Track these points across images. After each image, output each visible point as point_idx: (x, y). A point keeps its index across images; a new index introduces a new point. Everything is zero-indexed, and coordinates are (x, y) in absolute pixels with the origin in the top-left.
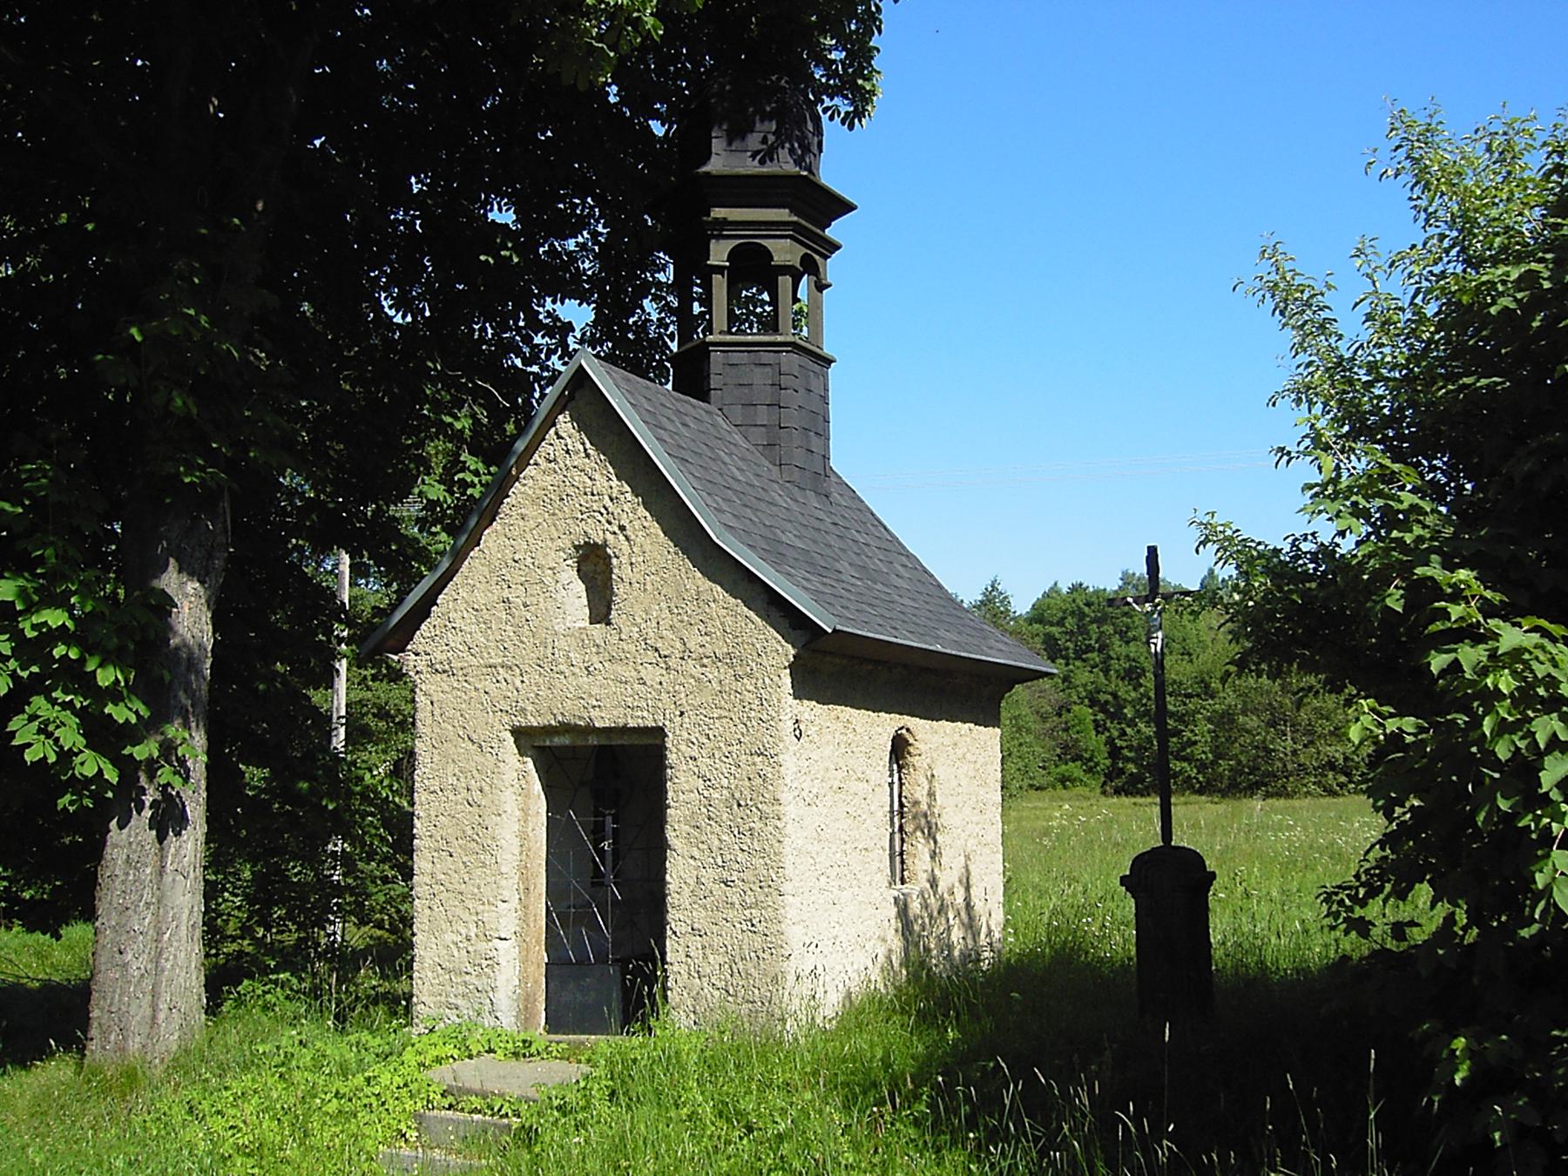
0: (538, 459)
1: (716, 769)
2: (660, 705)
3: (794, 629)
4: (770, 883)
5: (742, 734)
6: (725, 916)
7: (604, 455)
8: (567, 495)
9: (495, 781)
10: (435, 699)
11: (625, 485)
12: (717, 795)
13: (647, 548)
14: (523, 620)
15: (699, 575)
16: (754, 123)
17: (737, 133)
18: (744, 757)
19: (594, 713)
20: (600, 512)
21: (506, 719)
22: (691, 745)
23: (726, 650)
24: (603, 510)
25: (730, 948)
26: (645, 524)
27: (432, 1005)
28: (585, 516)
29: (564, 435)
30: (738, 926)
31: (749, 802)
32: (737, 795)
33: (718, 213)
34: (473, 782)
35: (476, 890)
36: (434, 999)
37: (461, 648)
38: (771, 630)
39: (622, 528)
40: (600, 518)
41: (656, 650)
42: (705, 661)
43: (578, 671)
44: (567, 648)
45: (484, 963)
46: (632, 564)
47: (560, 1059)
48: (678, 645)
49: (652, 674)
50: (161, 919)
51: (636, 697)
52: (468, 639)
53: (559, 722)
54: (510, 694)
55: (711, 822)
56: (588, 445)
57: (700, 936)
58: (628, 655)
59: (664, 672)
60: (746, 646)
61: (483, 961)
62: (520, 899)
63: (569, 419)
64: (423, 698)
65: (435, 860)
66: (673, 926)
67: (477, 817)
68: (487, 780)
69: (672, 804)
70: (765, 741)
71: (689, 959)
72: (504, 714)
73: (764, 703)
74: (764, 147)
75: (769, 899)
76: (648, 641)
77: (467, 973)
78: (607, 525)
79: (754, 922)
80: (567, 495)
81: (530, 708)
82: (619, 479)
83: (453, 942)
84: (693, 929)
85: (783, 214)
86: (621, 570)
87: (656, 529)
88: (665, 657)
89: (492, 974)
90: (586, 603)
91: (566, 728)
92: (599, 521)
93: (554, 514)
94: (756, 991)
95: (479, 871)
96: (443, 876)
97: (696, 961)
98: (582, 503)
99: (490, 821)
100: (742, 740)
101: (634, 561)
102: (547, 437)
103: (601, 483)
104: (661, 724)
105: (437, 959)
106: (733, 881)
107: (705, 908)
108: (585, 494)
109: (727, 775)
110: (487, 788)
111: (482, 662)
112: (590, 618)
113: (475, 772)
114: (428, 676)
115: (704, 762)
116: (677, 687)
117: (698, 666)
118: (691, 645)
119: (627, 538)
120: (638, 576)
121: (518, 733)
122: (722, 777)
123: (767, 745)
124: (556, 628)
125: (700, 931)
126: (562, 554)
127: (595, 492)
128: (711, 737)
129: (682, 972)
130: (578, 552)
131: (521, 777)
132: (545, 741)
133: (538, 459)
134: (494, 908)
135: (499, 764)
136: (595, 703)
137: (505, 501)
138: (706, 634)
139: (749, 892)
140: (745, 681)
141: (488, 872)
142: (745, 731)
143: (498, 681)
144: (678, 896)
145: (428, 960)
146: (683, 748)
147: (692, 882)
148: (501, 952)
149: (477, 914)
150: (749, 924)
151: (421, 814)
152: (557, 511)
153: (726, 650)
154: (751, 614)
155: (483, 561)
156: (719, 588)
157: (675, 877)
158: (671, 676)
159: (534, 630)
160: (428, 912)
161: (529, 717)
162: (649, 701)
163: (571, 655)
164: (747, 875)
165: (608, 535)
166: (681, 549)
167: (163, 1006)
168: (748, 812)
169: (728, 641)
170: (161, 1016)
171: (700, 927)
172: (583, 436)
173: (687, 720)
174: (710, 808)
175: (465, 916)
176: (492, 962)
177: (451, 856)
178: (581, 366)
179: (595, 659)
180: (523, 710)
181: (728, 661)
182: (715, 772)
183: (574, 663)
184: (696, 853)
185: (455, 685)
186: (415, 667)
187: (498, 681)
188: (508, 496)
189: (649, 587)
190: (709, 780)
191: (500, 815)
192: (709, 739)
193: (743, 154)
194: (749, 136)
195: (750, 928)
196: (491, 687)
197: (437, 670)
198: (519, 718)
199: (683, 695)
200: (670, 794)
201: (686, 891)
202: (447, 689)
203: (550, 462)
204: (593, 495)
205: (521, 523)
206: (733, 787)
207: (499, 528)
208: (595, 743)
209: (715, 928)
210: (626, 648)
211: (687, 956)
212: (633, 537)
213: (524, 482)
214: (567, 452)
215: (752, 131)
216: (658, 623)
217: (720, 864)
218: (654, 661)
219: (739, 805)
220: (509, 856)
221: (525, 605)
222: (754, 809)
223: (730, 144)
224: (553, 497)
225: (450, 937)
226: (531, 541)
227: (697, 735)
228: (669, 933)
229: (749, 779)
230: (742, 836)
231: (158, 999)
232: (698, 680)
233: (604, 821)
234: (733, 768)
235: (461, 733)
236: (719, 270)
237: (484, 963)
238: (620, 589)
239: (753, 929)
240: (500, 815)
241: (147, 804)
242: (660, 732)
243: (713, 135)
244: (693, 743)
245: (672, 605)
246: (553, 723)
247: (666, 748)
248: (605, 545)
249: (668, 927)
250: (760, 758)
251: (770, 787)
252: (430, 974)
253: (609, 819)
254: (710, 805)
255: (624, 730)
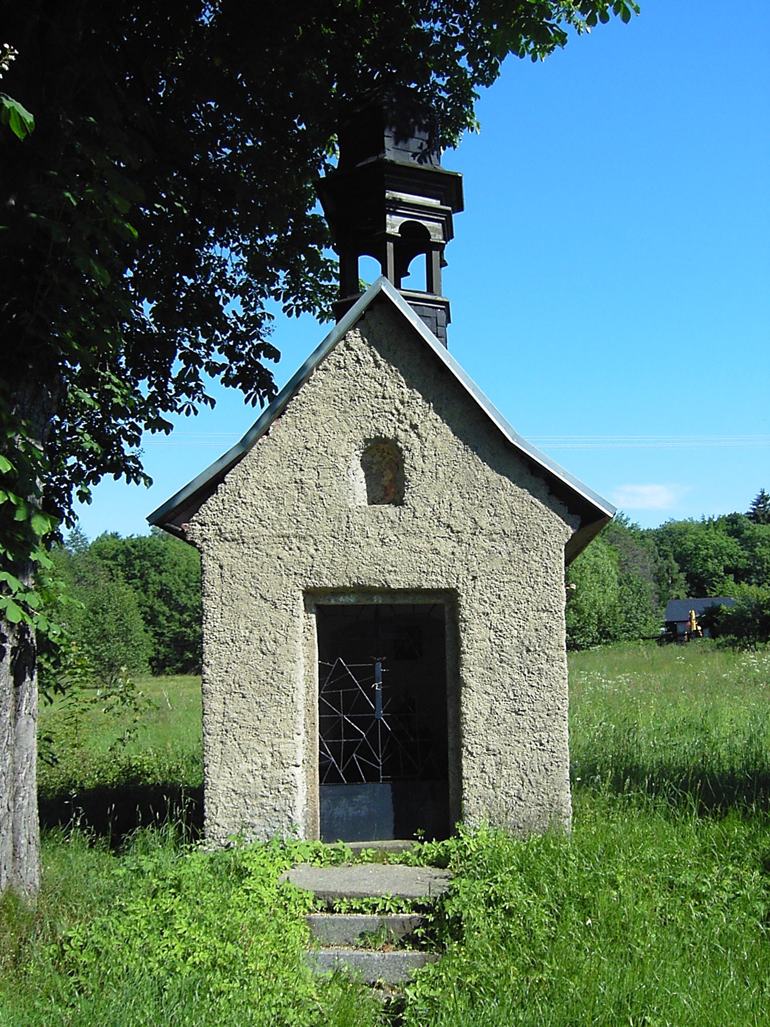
0: (327, 365)
1: (507, 623)
2: (454, 571)
3: (572, 514)
4: (557, 711)
5: (530, 594)
6: (517, 738)
7: (395, 366)
8: (359, 397)
9: (290, 633)
10: (224, 563)
11: (417, 393)
12: (507, 643)
13: (439, 444)
14: (317, 498)
15: (487, 468)
16: (414, 132)
17: (402, 137)
18: (531, 612)
19: (390, 577)
20: (391, 413)
21: (300, 581)
22: (484, 604)
23: (514, 528)
24: (394, 411)
25: (522, 763)
26: (436, 425)
27: (226, 826)
28: (376, 415)
29: (355, 347)
30: (528, 745)
31: (537, 648)
32: (527, 643)
33: (389, 194)
34: (267, 634)
35: (271, 726)
36: (228, 820)
37: (252, 520)
38: (554, 514)
39: (414, 427)
40: (391, 417)
41: (449, 526)
42: (494, 536)
43: (372, 542)
44: (362, 523)
45: (282, 787)
46: (424, 456)
47: (372, 862)
48: (469, 523)
49: (446, 547)
50: (16, 760)
51: (431, 564)
52: (259, 512)
53: (354, 584)
54: (304, 560)
55: (503, 665)
56: (379, 357)
57: (494, 755)
58: (422, 530)
59: (456, 545)
60: (532, 526)
61: (281, 785)
62: (307, 732)
63: (359, 335)
64: (210, 563)
65: (227, 701)
66: (470, 748)
67: (271, 663)
68: (282, 632)
69: (467, 650)
70: (551, 600)
71: (484, 774)
72: (298, 577)
73: (549, 570)
74: (420, 151)
75: (556, 723)
76: (441, 519)
77: (263, 796)
78: (397, 424)
79: (543, 742)
80: (359, 397)
81: (325, 571)
82: (410, 386)
83: (249, 771)
84: (488, 750)
85: (435, 203)
86: (413, 461)
87: (446, 429)
88: (458, 532)
89: (289, 796)
90: (365, 488)
91: (360, 589)
92: (391, 420)
93: (345, 412)
94: (545, 797)
95: (273, 710)
96: (236, 715)
97: (490, 775)
98: (373, 404)
99: (286, 667)
100: (530, 599)
101: (426, 453)
102: (337, 347)
103: (392, 389)
104: (454, 587)
105: (231, 786)
106: (524, 711)
107: (498, 733)
108: (376, 397)
109: (516, 627)
110: (282, 640)
111: (274, 532)
112: (368, 499)
113: (269, 626)
114: (216, 543)
115: (495, 617)
116: (469, 557)
117: (487, 541)
118: (483, 523)
119: (419, 436)
120: (430, 466)
121: (310, 594)
122: (513, 628)
123: (553, 604)
124: (350, 507)
125: (494, 751)
126: (353, 445)
127: (387, 396)
128: (502, 596)
129: (478, 784)
130: (366, 444)
131: (306, 630)
132: (330, 600)
133: (327, 365)
134: (290, 740)
135: (293, 619)
136: (391, 568)
137: (295, 398)
138: (495, 515)
139: (539, 719)
140: (532, 553)
141: (283, 710)
142: (532, 592)
143: (290, 549)
144: (474, 724)
145: (221, 787)
146: (476, 605)
147: (486, 713)
148: (297, 777)
149: (272, 745)
150: (538, 744)
151: (211, 662)
152: (348, 410)
153: (514, 528)
154: (536, 501)
155: (274, 447)
156: (507, 479)
157: (471, 708)
158: (463, 548)
159: (328, 507)
160: (220, 746)
161: (325, 580)
162: (443, 568)
163: (367, 528)
164: (538, 706)
165: (399, 432)
166: (470, 447)
167: (24, 841)
168: (537, 656)
169: (516, 521)
170: (24, 850)
171: (495, 748)
172: (374, 349)
173: (479, 583)
174: (502, 654)
175: (260, 748)
176: (291, 787)
177: (244, 697)
178: (382, 291)
179: (390, 532)
180: (318, 574)
181: (515, 537)
182: (505, 624)
183: (369, 535)
184: (490, 690)
185: (246, 552)
186: (201, 535)
187: (290, 549)
188: (298, 394)
189: (441, 475)
190: (501, 631)
191: (295, 662)
192: (500, 598)
193: (406, 153)
194: (410, 140)
195: (539, 746)
196: (284, 554)
197: (226, 539)
198: (313, 580)
199: (475, 564)
200: (465, 642)
201: (482, 720)
202: (236, 554)
203: (340, 368)
204: (384, 397)
205: (312, 418)
206: (522, 636)
207: (289, 420)
208: (380, 602)
209: (508, 748)
210: (420, 524)
211: (482, 771)
212: (425, 435)
213: (314, 383)
214: (358, 361)
215: (413, 137)
216: (451, 505)
217: (512, 697)
218: (447, 536)
219: (528, 651)
220: (300, 697)
221: (318, 486)
222: (541, 654)
223: (396, 143)
224: (344, 398)
225: (244, 767)
226: (323, 433)
227: (488, 595)
228: (465, 753)
229: (537, 630)
230: (531, 675)
231: (19, 834)
232: (489, 552)
233: (374, 667)
234: (521, 621)
235: (253, 593)
236: (391, 238)
237: (282, 787)
238: (414, 477)
239: (542, 747)
240: (295, 662)
241: (9, 651)
242: (450, 596)
243: (386, 134)
244: (486, 602)
245: (464, 491)
246: (348, 585)
247: (460, 606)
248: (396, 439)
249: (464, 750)
250: (545, 614)
251: (555, 636)
252: (223, 799)
253: (379, 665)
254: (503, 651)
255: (419, 591)
